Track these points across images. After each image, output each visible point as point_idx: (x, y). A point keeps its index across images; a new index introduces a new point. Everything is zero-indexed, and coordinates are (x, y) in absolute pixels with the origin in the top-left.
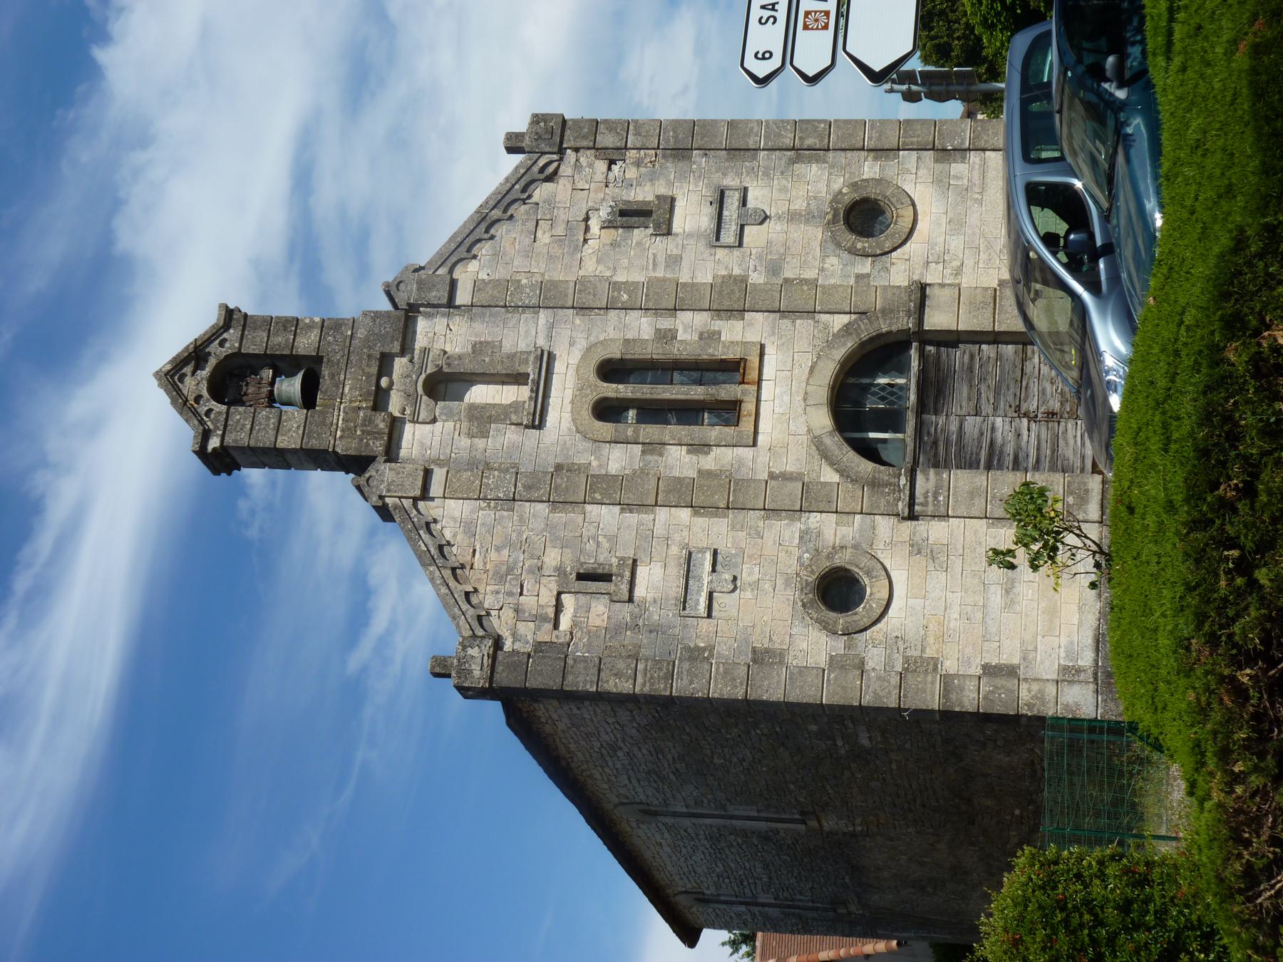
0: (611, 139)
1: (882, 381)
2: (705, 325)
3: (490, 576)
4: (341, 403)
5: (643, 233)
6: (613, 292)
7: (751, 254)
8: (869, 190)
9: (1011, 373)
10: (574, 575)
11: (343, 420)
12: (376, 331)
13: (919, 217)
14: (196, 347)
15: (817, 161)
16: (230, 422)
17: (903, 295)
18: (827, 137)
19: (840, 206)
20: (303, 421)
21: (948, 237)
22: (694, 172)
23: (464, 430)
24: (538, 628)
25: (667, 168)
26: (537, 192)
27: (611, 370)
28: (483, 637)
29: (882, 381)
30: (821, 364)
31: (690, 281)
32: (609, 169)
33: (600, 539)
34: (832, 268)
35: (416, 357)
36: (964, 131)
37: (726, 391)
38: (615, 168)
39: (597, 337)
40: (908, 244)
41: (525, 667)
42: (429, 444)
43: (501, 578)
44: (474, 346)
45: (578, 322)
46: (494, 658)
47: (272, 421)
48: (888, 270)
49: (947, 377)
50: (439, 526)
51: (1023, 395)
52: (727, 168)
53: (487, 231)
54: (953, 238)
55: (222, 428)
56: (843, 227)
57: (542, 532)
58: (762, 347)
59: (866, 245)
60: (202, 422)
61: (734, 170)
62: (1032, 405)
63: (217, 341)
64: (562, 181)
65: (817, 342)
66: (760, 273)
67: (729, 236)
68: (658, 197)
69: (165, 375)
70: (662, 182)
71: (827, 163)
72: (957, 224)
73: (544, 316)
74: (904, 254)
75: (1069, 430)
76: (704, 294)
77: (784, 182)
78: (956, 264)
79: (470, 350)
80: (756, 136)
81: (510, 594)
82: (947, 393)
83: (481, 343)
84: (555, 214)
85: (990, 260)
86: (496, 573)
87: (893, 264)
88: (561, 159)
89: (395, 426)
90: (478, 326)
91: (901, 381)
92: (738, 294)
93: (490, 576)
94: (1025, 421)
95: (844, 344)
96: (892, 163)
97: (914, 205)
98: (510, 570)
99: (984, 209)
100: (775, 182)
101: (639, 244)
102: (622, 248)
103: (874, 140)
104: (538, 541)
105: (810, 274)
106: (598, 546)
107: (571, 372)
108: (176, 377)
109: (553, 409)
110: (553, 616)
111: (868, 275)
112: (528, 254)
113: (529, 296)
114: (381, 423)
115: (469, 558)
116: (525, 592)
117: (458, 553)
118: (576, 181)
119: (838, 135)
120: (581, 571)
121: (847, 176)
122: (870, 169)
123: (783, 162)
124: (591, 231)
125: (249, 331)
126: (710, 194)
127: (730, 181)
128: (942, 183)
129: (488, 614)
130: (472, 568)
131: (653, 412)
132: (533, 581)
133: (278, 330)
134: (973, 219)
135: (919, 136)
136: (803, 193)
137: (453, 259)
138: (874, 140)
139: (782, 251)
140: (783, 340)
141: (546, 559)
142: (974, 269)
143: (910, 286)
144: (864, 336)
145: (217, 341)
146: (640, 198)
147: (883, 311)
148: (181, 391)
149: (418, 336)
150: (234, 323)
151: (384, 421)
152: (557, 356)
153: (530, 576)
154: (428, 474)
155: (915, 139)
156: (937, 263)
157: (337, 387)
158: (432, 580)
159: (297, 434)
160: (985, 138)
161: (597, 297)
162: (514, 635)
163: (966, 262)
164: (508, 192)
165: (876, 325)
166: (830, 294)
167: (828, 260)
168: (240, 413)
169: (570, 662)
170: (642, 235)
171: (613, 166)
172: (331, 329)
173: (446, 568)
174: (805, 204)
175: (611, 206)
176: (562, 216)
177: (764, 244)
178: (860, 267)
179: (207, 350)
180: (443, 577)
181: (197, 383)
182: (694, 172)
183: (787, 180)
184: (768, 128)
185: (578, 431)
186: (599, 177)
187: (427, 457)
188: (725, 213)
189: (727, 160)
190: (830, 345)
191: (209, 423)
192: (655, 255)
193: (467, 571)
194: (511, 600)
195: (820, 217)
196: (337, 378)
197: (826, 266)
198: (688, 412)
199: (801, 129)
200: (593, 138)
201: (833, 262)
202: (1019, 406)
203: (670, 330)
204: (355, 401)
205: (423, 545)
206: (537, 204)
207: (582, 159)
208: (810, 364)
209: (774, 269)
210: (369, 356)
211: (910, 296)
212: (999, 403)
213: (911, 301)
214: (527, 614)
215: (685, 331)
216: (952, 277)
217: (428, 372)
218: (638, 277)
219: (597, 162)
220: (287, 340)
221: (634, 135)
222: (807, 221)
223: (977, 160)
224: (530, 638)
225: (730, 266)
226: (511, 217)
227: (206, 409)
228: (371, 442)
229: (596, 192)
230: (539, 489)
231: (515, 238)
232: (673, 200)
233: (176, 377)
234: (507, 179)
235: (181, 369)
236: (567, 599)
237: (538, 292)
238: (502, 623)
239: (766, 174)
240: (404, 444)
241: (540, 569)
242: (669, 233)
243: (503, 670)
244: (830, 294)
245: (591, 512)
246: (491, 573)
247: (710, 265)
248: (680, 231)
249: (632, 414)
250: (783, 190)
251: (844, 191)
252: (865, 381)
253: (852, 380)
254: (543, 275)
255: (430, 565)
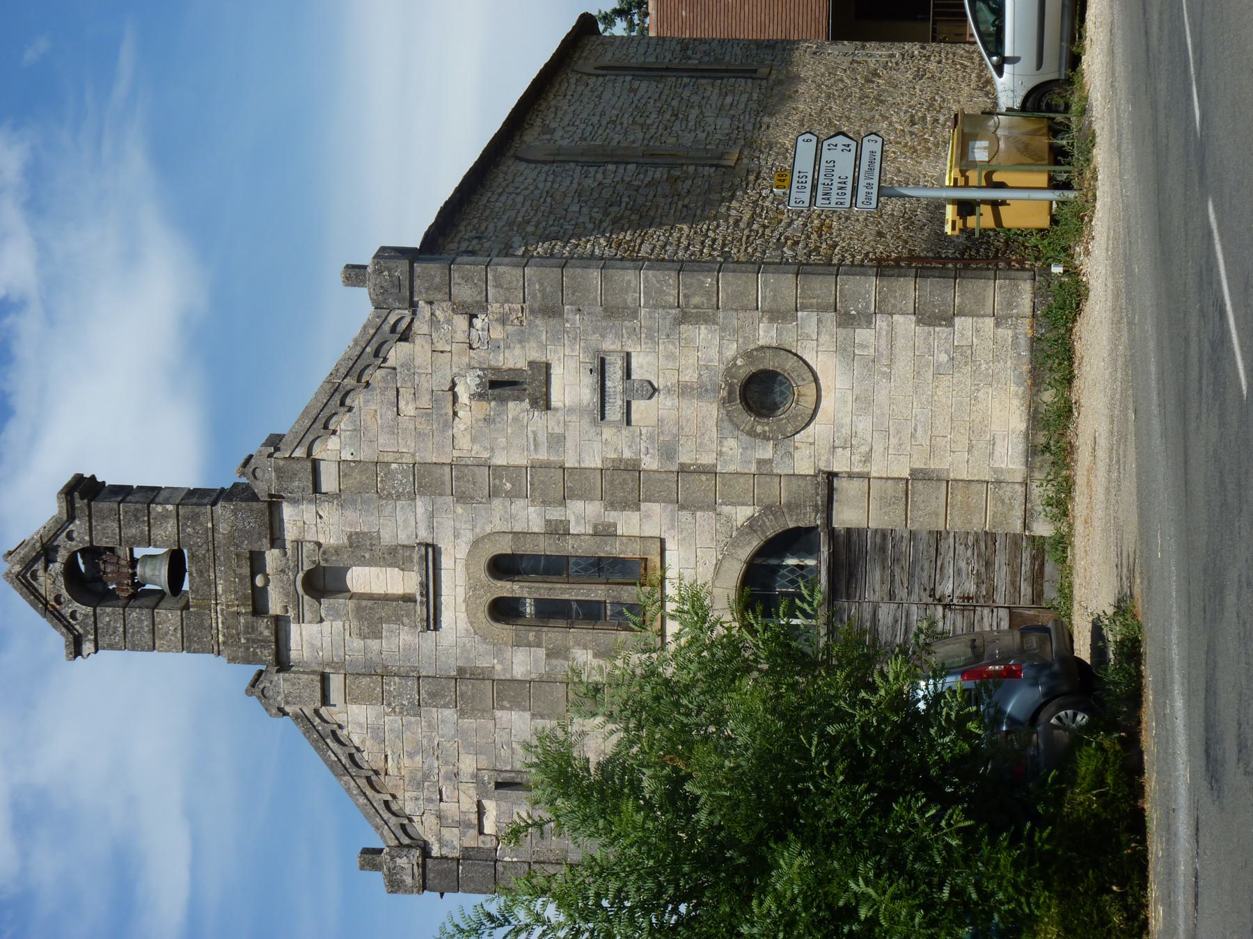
0: (469, 292)
1: (791, 562)
2: (599, 516)
3: (407, 782)
4: (217, 604)
5: (519, 407)
6: (494, 479)
7: (641, 434)
8: (766, 362)
9: (925, 553)
10: (492, 784)
11: (223, 623)
12: (241, 527)
13: (823, 393)
14: (43, 545)
15: (706, 322)
16: (99, 625)
17: (809, 487)
18: (715, 295)
19: (735, 381)
20: (179, 624)
21: (854, 417)
22: (568, 333)
23: (355, 631)
24: (463, 834)
25: (537, 326)
26: (392, 353)
27: (502, 567)
28: (409, 846)
29: (791, 562)
30: (726, 565)
31: (577, 465)
32: (471, 325)
33: (514, 745)
34: (730, 452)
35: (289, 552)
36: (868, 292)
37: (629, 594)
38: (478, 323)
39: (483, 529)
40: (812, 425)
41: (455, 873)
42: (320, 645)
43: (419, 785)
44: (350, 537)
45: (459, 510)
46: (424, 866)
47: (146, 623)
48: (791, 456)
49: (859, 559)
50: (345, 732)
51: (938, 577)
52: (605, 329)
53: (342, 404)
54: (860, 418)
55: (92, 632)
56: (740, 406)
57: (453, 738)
58: (662, 541)
59: (767, 428)
60: (70, 628)
61: (613, 331)
62: (946, 588)
63: (64, 534)
64: (418, 340)
65: (721, 537)
66: (653, 457)
67: (615, 411)
68: (531, 364)
69: (17, 577)
70: (533, 344)
71: (717, 324)
72: (864, 402)
73: (421, 505)
74: (808, 437)
75: (985, 620)
76: (594, 483)
77: (671, 347)
78: (865, 449)
79: (346, 541)
80: (635, 292)
81: (430, 800)
82: (859, 576)
83: (357, 533)
84: (416, 382)
85: (901, 445)
86: (412, 779)
87: (796, 448)
88: (414, 313)
89: (280, 625)
90: (350, 515)
91: (810, 562)
92: (631, 485)
93: (407, 782)
94: (940, 609)
95: (749, 543)
96: (790, 326)
97: (816, 380)
98: (426, 777)
99: (892, 384)
100: (661, 347)
101: (516, 419)
102: (498, 425)
103: (768, 300)
104: (450, 746)
105: (707, 459)
106: (513, 753)
107: (460, 567)
108: (28, 575)
109: (447, 609)
110: (476, 822)
111: (770, 461)
112: (393, 430)
113: (402, 484)
114: (265, 629)
115: (382, 764)
116: (444, 797)
117: (369, 757)
118: (435, 340)
119: (727, 293)
120: (499, 780)
121: (741, 341)
122: (766, 334)
123: (668, 322)
124: (460, 400)
125: (96, 521)
126: (589, 361)
127: (608, 345)
128: (846, 352)
129: (411, 820)
130: (386, 774)
131: (551, 612)
132: (451, 787)
133: (129, 521)
134: (881, 396)
135: (818, 297)
136: (692, 360)
137: (310, 437)
138: (768, 300)
139: (675, 431)
140: (684, 534)
141: (462, 766)
142: (884, 455)
143: (815, 476)
144: (770, 534)
145: (64, 534)
146: (510, 364)
147: (789, 505)
148: (37, 590)
149: (286, 525)
150: (77, 512)
151: (267, 627)
152: (443, 549)
153: (448, 782)
154: (324, 679)
155: (814, 301)
156: (844, 448)
157: (209, 586)
158: (348, 790)
159: (176, 637)
160: (892, 301)
161: (477, 485)
162: (440, 840)
163: (874, 447)
164: (359, 357)
165: (782, 522)
166: (730, 486)
167: (725, 443)
168: (108, 615)
169: (500, 868)
170: (518, 409)
171: (474, 320)
172: (188, 519)
173: (360, 777)
174: (696, 375)
175: (479, 376)
176: (425, 384)
177: (654, 422)
178: (761, 451)
179: (55, 544)
180: (359, 787)
181: (50, 580)
182: (568, 333)
183: (673, 344)
184: (648, 282)
185: (476, 633)
186: (460, 336)
187: (320, 659)
188: (608, 384)
189: (604, 318)
190: (734, 543)
191: (77, 627)
192: (535, 433)
193: (382, 777)
194: (431, 806)
195: (714, 390)
196: (206, 575)
197: (724, 449)
198: (591, 613)
199: (685, 285)
200: (447, 290)
201: (731, 445)
202: (934, 589)
203: (561, 521)
204: (233, 606)
205: (332, 755)
206: (395, 369)
207: (438, 313)
208: (714, 562)
209: (668, 452)
210: (238, 555)
211: (817, 488)
212: (913, 587)
213: (818, 495)
214: (450, 821)
215: (578, 523)
216: (861, 465)
217: (306, 568)
218: (520, 459)
219: (455, 317)
220: (142, 532)
221: (496, 287)
222: (700, 397)
223: (884, 325)
224: (456, 843)
225: (619, 447)
226: (368, 384)
227: (70, 610)
228: (258, 651)
229: (460, 355)
230: (444, 697)
231: (376, 411)
232: (548, 366)
233: (28, 575)
234: (356, 342)
235: (32, 566)
236: (490, 805)
237: (411, 479)
238: (426, 829)
239: (650, 337)
240: (293, 645)
241: (456, 775)
242: (548, 407)
243: (435, 877)
244: (730, 486)
245: (501, 718)
246: (407, 779)
247: (597, 446)
248: (560, 404)
249: (529, 609)
250: (670, 357)
251: (739, 362)
252: (774, 562)
253: (758, 561)
254: (413, 455)
255: (344, 775)
